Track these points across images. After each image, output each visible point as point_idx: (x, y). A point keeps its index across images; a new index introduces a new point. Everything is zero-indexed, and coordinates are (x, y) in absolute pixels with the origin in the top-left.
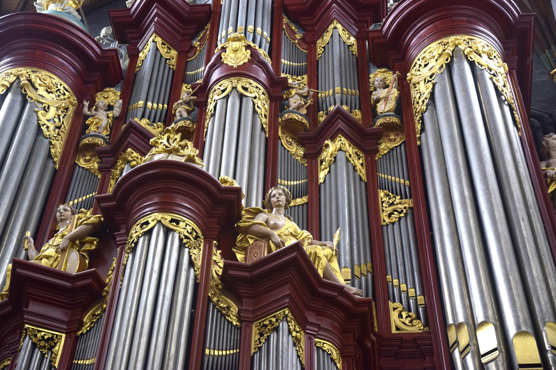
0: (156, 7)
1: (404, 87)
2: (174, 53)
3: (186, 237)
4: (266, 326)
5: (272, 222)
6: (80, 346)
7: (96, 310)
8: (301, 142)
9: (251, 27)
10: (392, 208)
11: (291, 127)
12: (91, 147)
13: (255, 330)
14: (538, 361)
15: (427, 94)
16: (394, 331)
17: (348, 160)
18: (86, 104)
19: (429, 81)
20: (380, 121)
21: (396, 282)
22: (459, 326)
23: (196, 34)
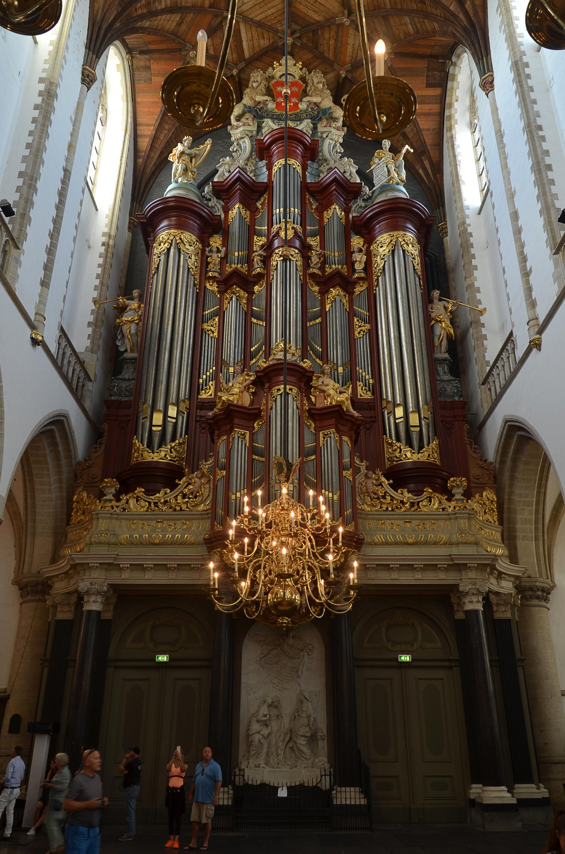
0: (239, 184)
1: (369, 254)
2: (248, 212)
3: (296, 397)
4: (326, 435)
5: (325, 383)
6: (255, 437)
7: (259, 422)
8: (318, 284)
9: (292, 209)
10: (361, 328)
11: (313, 275)
12: (213, 278)
13: (321, 435)
14: (418, 425)
16: (359, 397)
17: (341, 301)
19: (383, 259)
20: (356, 275)
21: (360, 371)
22: (388, 402)
23: (258, 199)
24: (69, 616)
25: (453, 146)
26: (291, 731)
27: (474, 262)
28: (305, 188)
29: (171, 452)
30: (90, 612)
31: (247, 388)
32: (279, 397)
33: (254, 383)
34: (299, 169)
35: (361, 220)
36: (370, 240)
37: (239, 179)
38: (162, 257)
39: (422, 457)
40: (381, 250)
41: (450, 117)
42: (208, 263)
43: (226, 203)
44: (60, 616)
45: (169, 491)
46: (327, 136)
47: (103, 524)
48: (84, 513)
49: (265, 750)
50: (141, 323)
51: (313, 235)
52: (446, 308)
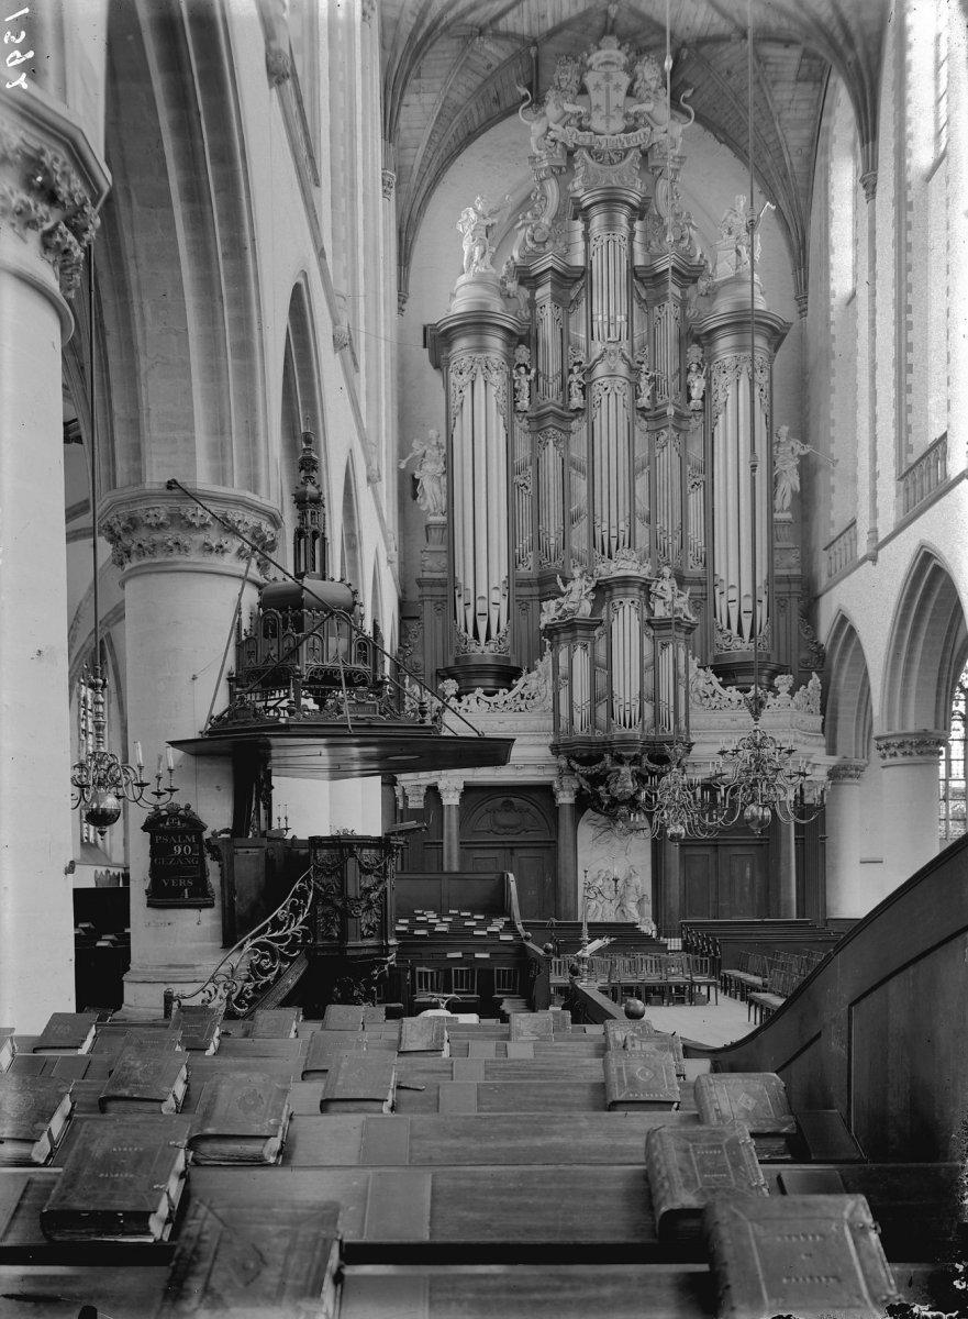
1: (708, 378)
9: (618, 317)
11: (643, 409)
18: (514, 372)
28: (633, 272)
37: (552, 268)
38: (467, 393)
40: (725, 376)
42: (516, 390)
43: (533, 295)
45: (506, 691)
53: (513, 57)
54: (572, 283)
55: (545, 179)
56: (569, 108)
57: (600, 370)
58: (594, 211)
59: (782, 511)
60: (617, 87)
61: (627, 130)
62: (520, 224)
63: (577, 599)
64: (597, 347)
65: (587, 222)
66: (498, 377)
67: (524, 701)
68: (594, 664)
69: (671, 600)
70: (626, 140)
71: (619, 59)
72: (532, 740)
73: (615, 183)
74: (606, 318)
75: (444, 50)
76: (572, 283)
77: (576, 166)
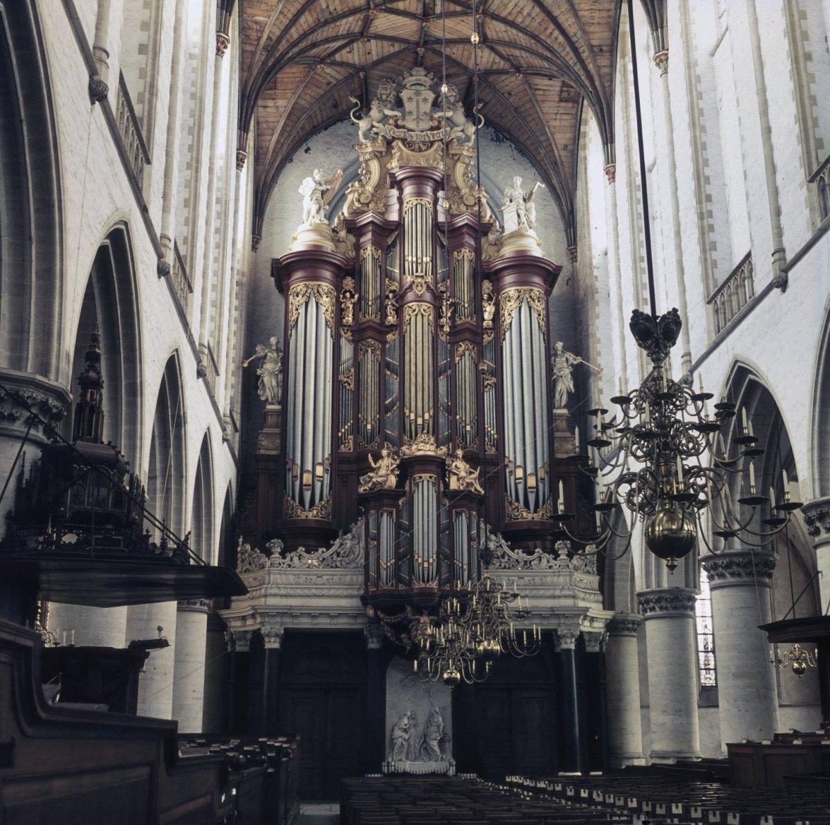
1: (497, 305)
2: (380, 251)
15: (509, 321)
18: (341, 296)
22: (510, 461)
24: (246, 649)
25: (586, 169)
26: (425, 735)
27: (597, 309)
28: (436, 226)
29: (322, 510)
30: (271, 650)
31: (393, 471)
32: (421, 484)
33: (398, 466)
34: (430, 207)
35: (491, 269)
36: (497, 289)
38: (302, 310)
39: (537, 517)
40: (509, 304)
41: (585, 134)
42: (342, 310)
43: (358, 240)
44: (238, 649)
45: (325, 550)
46: (458, 159)
47: (276, 577)
48: (250, 564)
49: (406, 750)
50: (280, 377)
51: (444, 280)
52: (567, 360)
53: (346, 79)
54: (389, 234)
55: (369, 160)
56: (388, 112)
57: (410, 296)
58: (406, 183)
59: (560, 407)
60: (425, 100)
61: (432, 129)
62: (350, 190)
63: (385, 472)
64: (408, 279)
65: (401, 190)
66: (327, 300)
67: (339, 559)
68: (399, 527)
69: (462, 475)
70: (431, 136)
71: (425, 82)
72: (346, 593)
73: (423, 164)
74: (414, 259)
75: (290, 75)
76: (389, 234)
77: (393, 151)
